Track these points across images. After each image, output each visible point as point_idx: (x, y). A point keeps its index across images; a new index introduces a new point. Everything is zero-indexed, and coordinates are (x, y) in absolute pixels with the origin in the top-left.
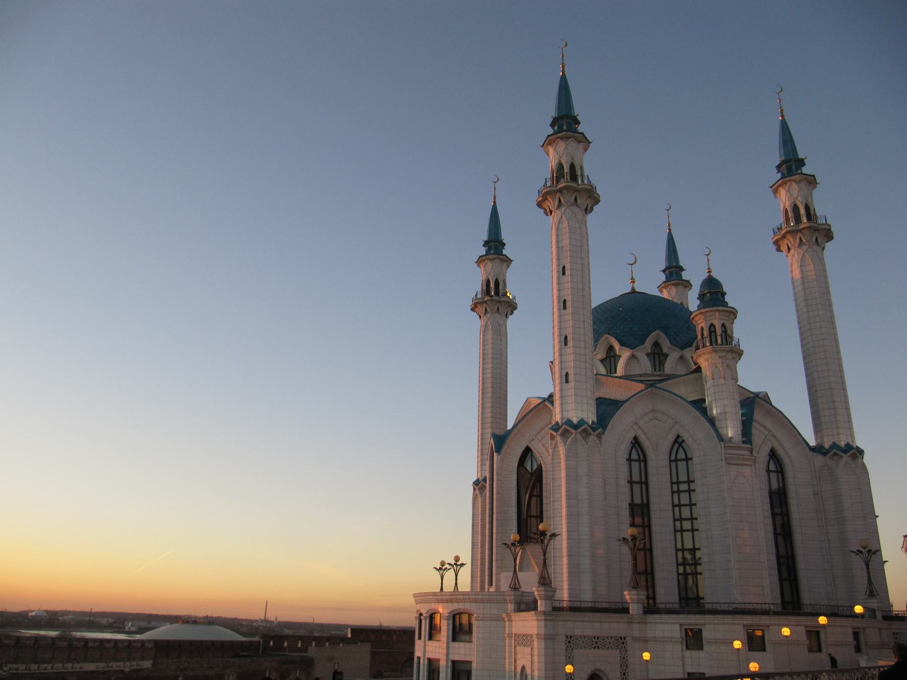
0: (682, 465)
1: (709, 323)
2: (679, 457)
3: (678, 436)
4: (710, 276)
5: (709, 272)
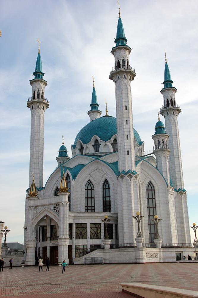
0: (150, 192)
1: (162, 139)
2: (149, 189)
3: (150, 181)
4: (159, 121)
5: (159, 119)
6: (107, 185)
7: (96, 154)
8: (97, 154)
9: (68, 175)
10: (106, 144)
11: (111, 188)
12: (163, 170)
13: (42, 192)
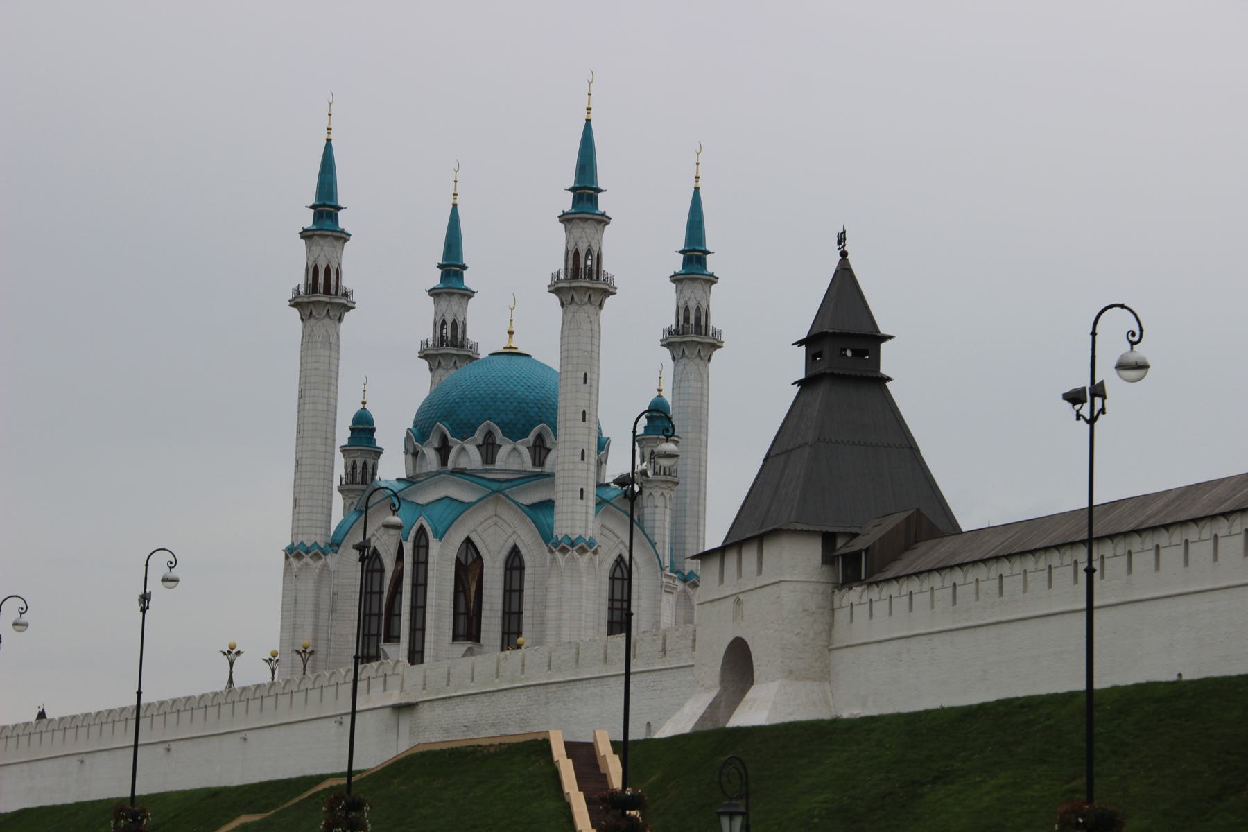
0: (618, 584)
6: (517, 559)
7: (487, 471)
8: (487, 471)
9: (422, 530)
10: (515, 449)
11: (528, 571)
12: (656, 530)
13: (331, 560)
